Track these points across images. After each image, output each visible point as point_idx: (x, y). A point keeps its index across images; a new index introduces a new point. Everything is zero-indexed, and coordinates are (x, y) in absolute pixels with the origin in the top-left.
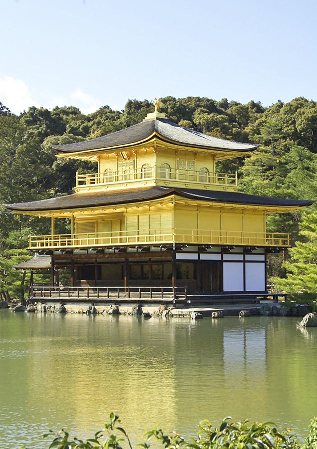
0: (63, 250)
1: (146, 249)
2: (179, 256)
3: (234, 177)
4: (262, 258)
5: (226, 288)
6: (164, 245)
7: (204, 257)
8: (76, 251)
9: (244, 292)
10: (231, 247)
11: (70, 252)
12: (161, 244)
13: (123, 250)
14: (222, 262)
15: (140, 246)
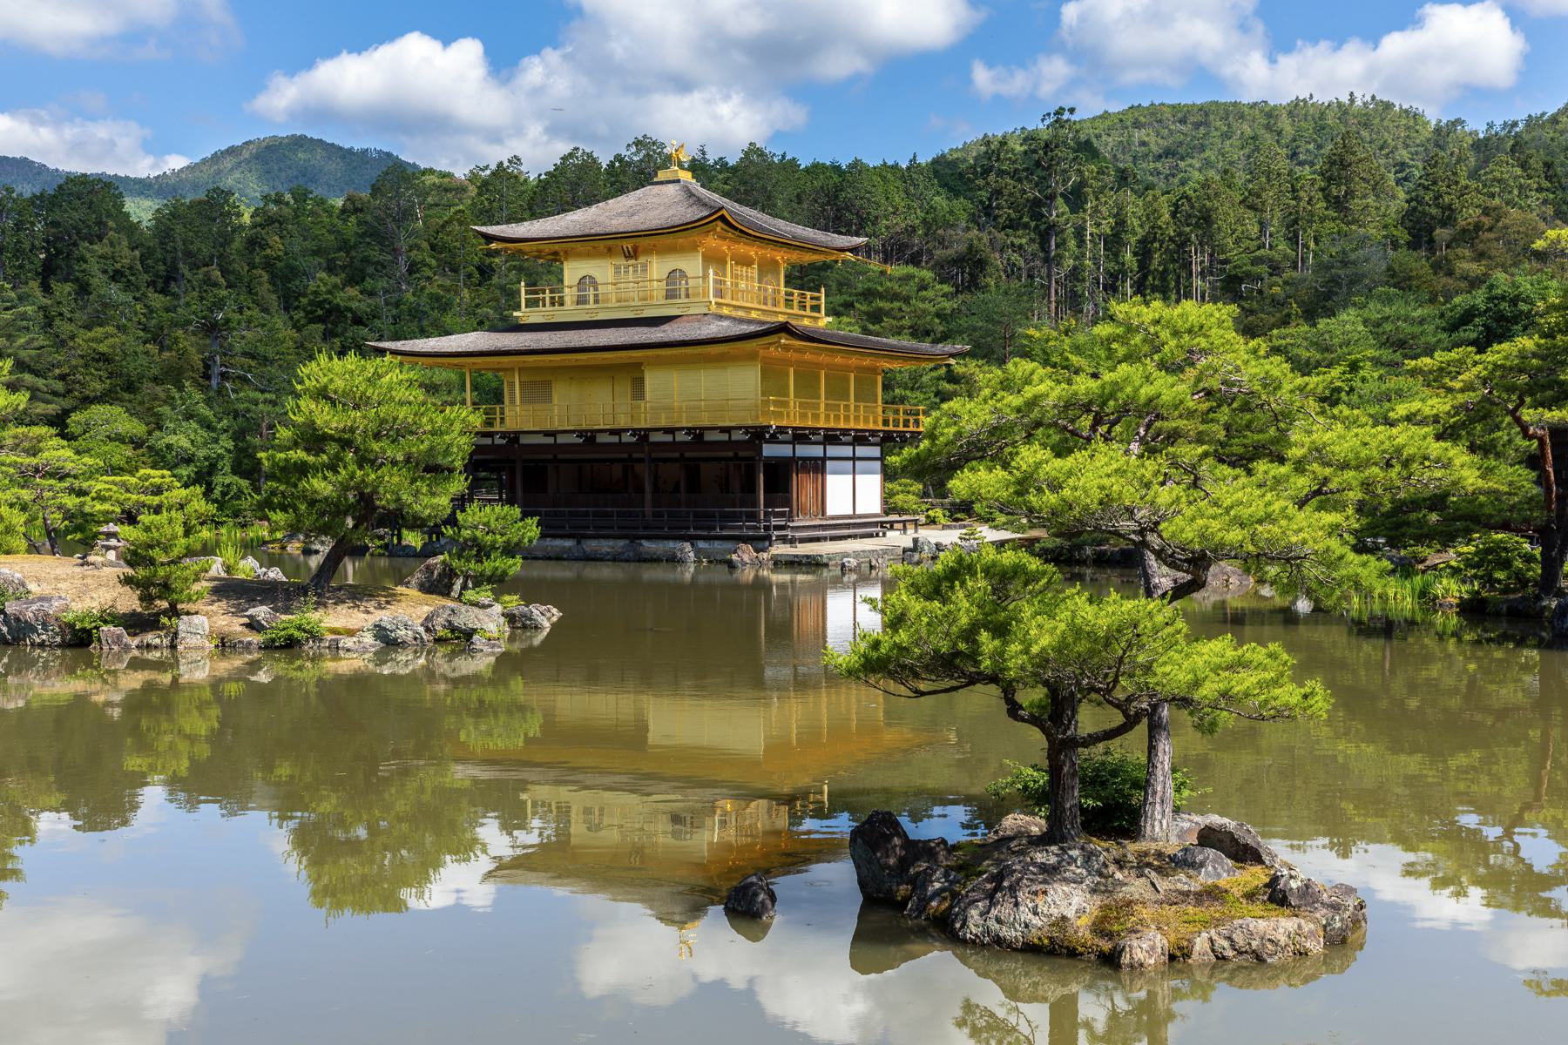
0: (504, 435)
1: (697, 433)
2: (769, 450)
3: (818, 299)
4: (875, 451)
5: (830, 511)
6: (747, 429)
7: (804, 451)
8: (524, 440)
9: (854, 516)
10: (845, 432)
11: (513, 437)
12: (740, 428)
13: (643, 435)
14: (824, 459)
15: (689, 430)
